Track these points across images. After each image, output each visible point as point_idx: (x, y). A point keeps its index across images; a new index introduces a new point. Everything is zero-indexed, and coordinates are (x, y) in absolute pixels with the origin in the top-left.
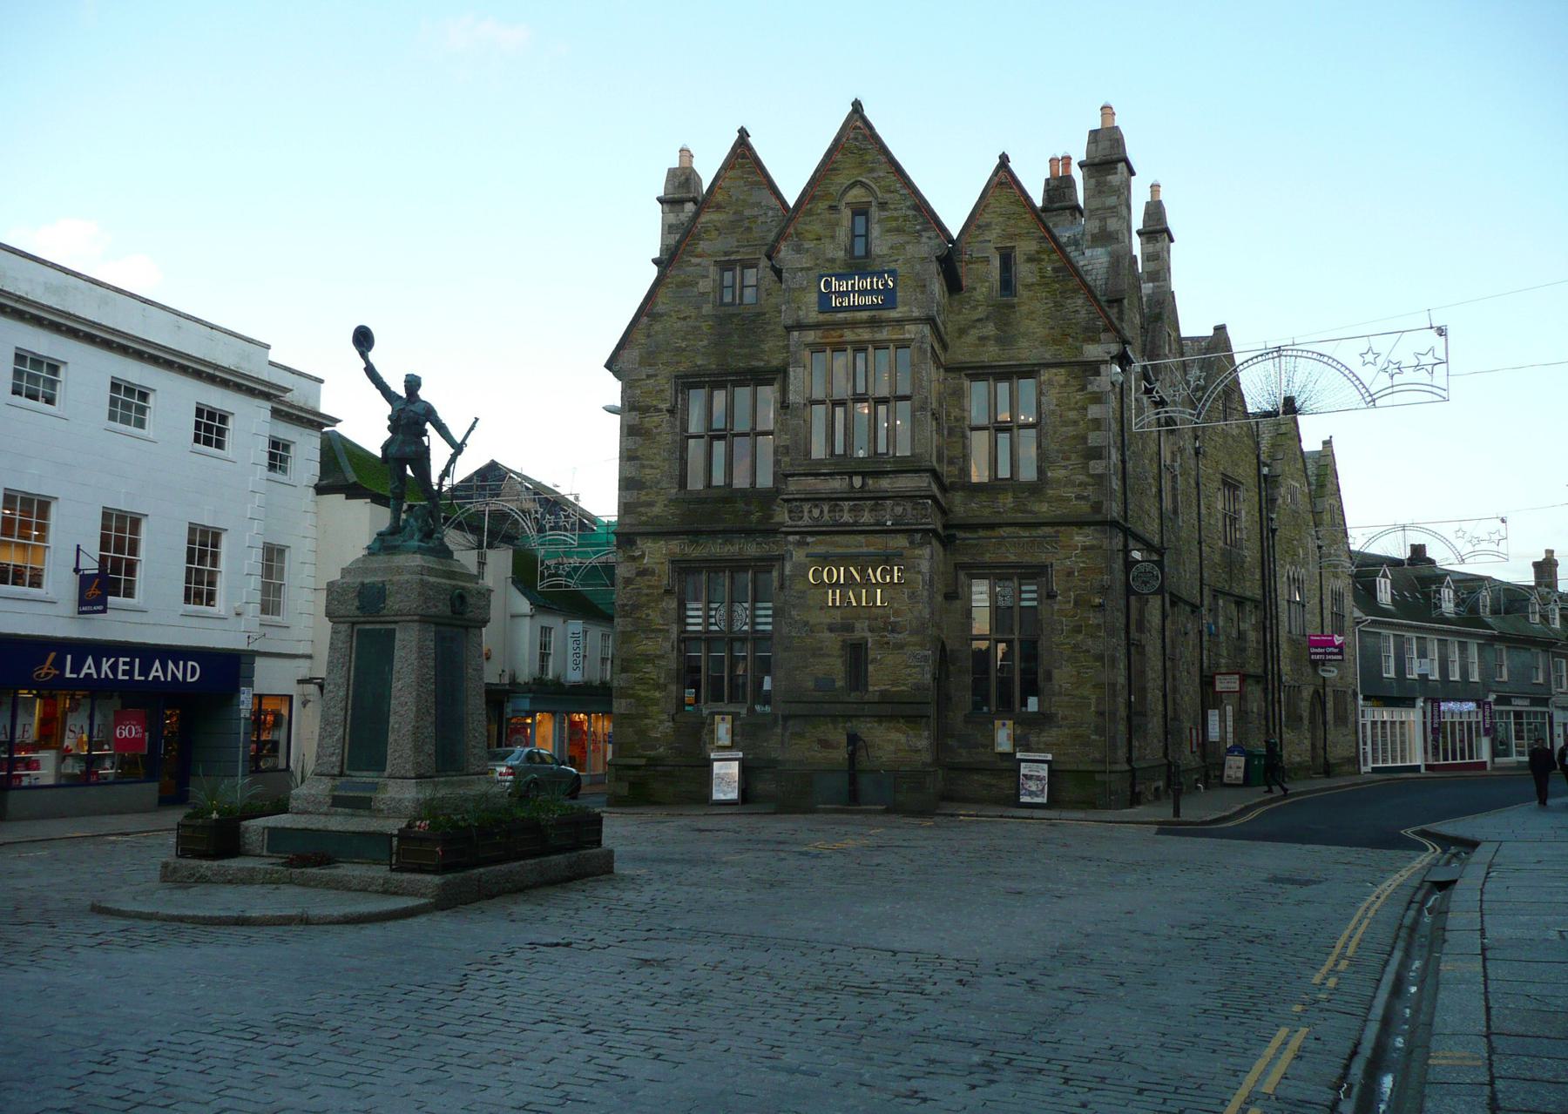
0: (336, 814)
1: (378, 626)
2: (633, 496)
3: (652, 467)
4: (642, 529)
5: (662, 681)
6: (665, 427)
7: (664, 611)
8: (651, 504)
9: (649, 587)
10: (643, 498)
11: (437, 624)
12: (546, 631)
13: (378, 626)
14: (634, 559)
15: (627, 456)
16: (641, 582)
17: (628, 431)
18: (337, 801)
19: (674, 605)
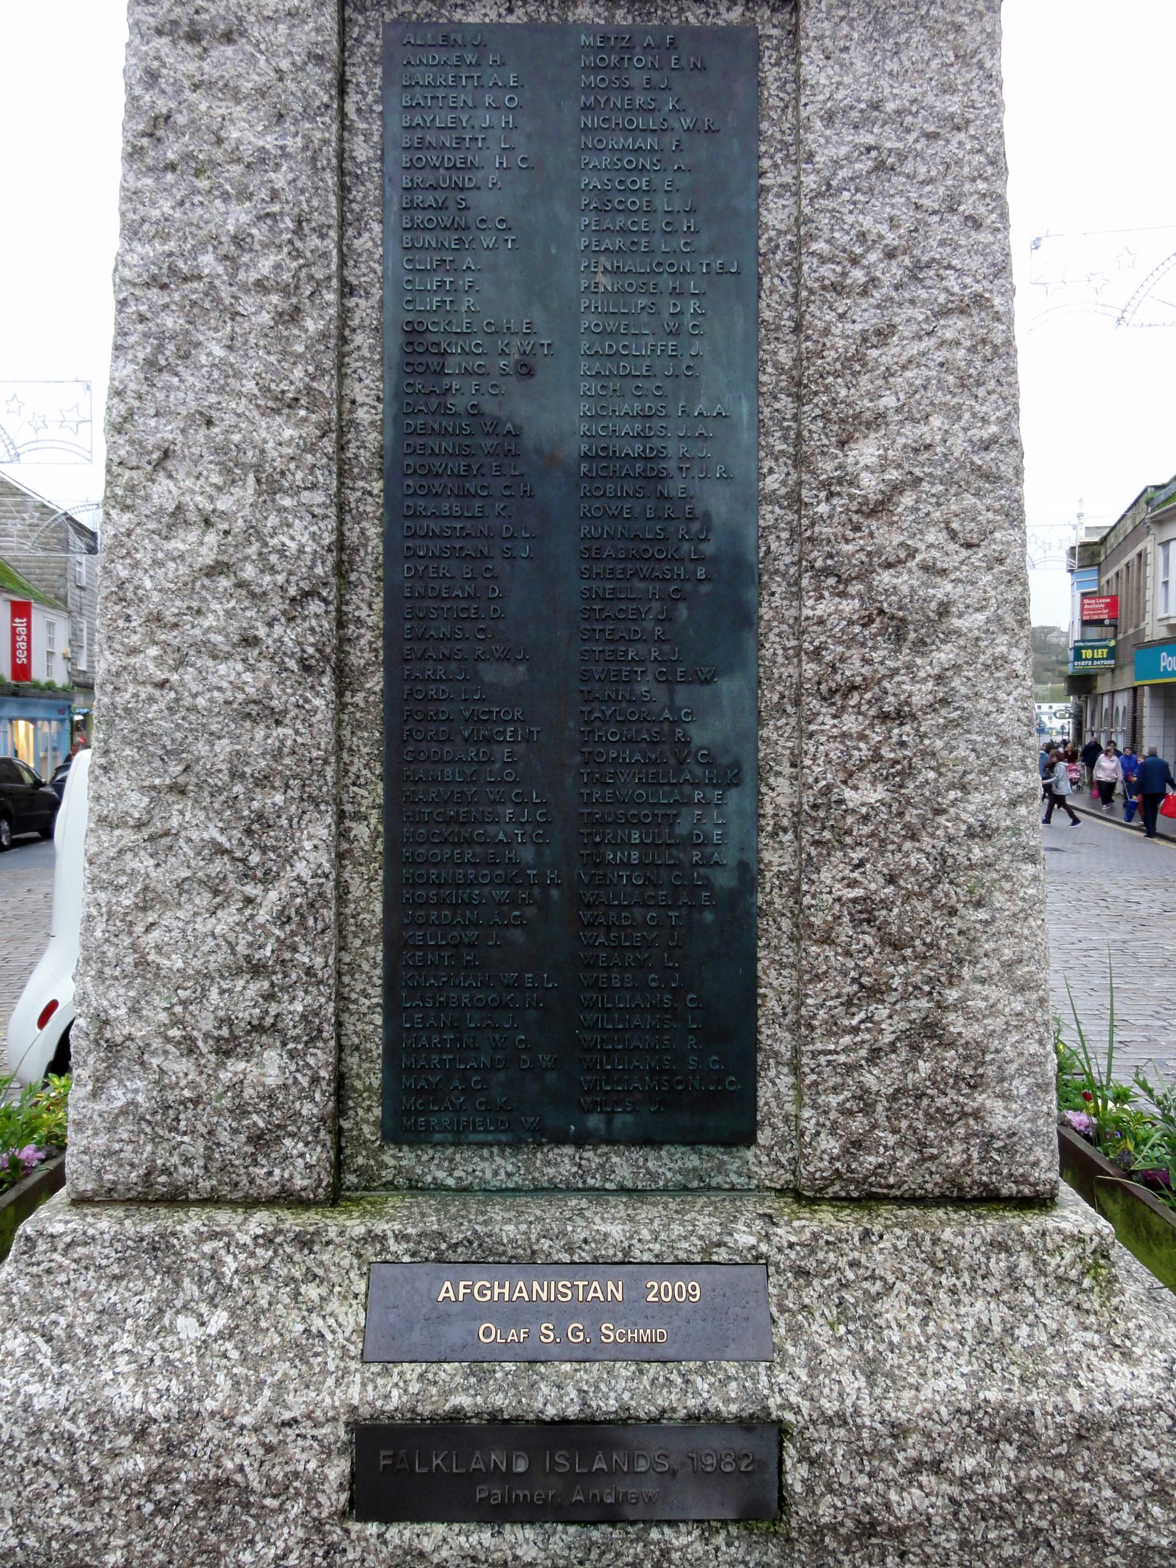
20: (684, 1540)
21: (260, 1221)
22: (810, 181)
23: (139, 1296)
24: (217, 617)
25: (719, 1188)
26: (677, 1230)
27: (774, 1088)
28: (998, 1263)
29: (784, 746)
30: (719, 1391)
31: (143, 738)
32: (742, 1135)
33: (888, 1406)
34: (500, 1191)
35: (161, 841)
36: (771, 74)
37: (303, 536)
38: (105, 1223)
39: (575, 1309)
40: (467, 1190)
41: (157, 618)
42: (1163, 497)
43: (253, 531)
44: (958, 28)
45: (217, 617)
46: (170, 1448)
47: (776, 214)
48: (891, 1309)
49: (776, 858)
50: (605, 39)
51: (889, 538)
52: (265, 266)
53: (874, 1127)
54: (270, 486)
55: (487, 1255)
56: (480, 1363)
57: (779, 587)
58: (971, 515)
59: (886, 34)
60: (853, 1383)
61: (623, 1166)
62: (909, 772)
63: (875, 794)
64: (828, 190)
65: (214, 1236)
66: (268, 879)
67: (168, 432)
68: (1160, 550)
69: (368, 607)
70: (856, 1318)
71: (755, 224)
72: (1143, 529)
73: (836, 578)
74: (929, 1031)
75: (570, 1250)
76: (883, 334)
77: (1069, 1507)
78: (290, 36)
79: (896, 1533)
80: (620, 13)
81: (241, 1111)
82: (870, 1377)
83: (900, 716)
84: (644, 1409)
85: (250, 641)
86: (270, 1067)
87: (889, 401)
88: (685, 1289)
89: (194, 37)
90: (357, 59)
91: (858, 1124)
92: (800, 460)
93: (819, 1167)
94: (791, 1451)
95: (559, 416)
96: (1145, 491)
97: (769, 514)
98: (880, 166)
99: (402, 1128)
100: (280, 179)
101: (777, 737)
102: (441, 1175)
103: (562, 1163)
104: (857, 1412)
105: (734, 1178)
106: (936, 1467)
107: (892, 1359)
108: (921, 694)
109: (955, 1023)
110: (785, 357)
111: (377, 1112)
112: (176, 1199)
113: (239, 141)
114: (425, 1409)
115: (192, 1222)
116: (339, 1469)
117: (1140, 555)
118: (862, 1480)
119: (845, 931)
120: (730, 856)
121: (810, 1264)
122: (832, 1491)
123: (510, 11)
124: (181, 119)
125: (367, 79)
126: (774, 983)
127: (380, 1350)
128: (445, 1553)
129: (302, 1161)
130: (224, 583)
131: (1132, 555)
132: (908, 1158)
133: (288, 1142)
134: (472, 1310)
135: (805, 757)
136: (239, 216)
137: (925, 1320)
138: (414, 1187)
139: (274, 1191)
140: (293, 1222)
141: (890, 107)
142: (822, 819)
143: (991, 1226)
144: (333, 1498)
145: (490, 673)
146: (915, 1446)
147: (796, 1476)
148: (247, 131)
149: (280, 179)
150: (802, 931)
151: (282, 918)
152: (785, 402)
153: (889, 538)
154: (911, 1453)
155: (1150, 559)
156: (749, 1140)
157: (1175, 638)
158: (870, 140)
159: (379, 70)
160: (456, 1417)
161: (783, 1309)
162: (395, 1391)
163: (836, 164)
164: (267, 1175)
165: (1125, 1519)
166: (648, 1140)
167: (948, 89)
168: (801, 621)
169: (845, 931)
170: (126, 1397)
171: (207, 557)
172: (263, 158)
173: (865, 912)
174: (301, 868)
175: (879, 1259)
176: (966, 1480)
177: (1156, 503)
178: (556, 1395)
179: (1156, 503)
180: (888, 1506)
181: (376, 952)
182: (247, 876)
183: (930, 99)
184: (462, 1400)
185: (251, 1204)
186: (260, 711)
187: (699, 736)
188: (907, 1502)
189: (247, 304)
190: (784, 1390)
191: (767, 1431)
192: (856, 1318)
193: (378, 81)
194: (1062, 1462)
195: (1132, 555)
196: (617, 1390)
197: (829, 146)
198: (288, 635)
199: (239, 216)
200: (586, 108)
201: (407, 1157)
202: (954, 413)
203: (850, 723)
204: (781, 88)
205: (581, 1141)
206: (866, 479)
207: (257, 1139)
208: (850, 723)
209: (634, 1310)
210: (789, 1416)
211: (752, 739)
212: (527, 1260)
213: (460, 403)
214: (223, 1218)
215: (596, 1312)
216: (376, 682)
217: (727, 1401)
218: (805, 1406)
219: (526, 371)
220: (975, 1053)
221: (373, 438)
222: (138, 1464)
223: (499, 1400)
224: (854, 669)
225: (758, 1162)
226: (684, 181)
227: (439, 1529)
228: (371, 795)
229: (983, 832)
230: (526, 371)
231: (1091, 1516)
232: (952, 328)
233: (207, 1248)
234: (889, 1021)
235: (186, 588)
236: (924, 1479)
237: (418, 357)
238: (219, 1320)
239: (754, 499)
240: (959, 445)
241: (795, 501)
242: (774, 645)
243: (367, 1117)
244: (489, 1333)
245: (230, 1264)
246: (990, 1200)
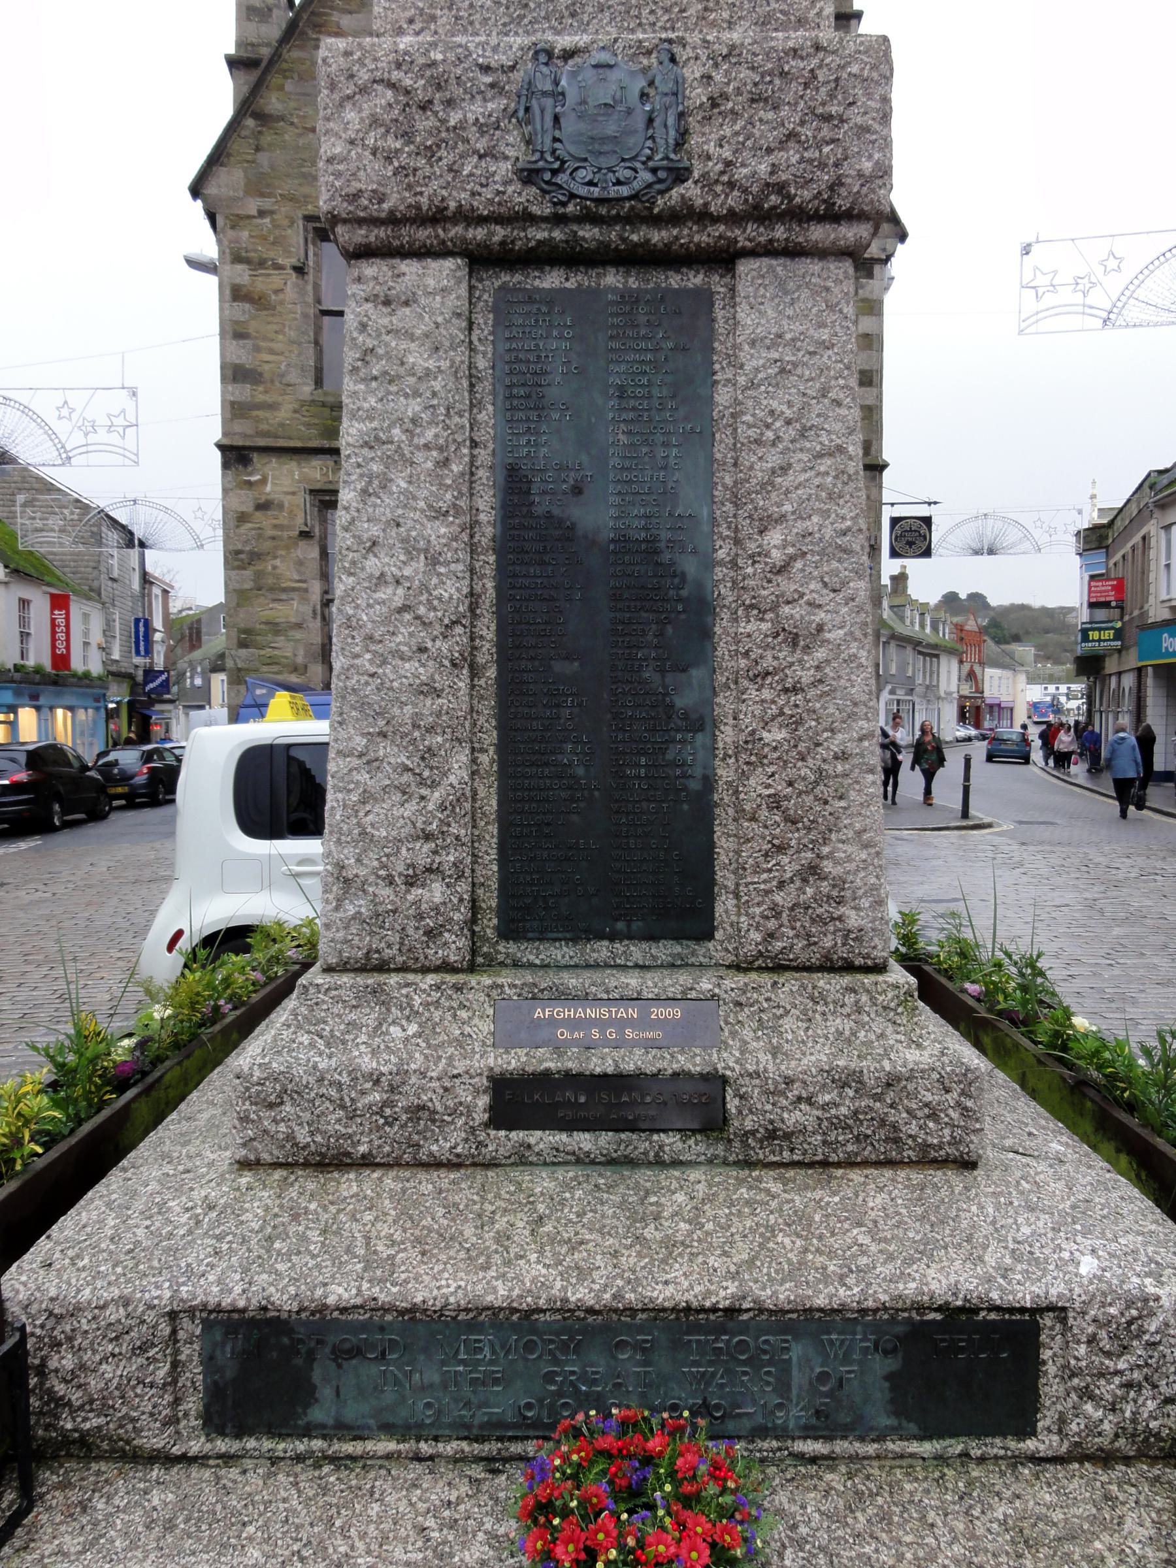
0: (522, 1159)
2: (244, 392)
3: (272, 352)
4: (262, 442)
5: (300, 660)
6: (290, 293)
7: (300, 563)
8: (273, 407)
9: (275, 526)
10: (261, 398)
12: (24, 603)
14: (250, 484)
15: (233, 332)
16: (264, 520)
17: (235, 294)
19: (315, 553)
20: (672, 1140)
21: (431, 979)
22: (742, 380)
23: (369, 1016)
24: (404, 635)
25: (693, 965)
26: (668, 982)
27: (724, 906)
28: (850, 999)
29: (730, 708)
30: (692, 1061)
31: (363, 705)
32: (706, 933)
33: (783, 1067)
34: (566, 967)
35: (373, 764)
36: (719, 314)
37: (451, 590)
38: (346, 979)
39: (611, 1022)
40: (548, 966)
41: (371, 638)
42: (1165, 482)
43: (424, 588)
44: (828, 289)
45: (404, 635)
46: (392, 1089)
47: (723, 396)
48: (787, 1023)
49: (725, 773)
50: (622, 297)
51: (788, 586)
52: (430, 434)
53: (781, 926)
54: (433, 561)
55: (562, 996)
56: (558, 1049)
57: (725, 615)
58: (836, 573)
59: (786, 293)
60: (765, 1058)
61: (637, 951)
62: (800, 722)
64: (752, 385)
65: (407, 985)
66: (434, 785)
67: (375, 531)
68: (1162, 533)
69: (487, 629)
70: (768, 1027)
71: (710, 401)
72: (1146, 513)
73: (757, 609)
74: (812, 871)
75: (608, 992)
76: (785, 469)
77: (883, 1122)
78: (443, 303)
79: (788, 1136)
80: (631, 280)
81: (420, 917)
82: (774, 1056)
83: (795, 690)
84: (650, 1069)
85: (422, 650)
86: (436, 892)
87: (788, 508)
88: (674, 1012)
89: (387, 302)
90: (478, 309)
91: (772, 924)
92: (737, 542)
93: (750, 949)
94: (729, 1092)
95: (598, 517)
96: (1149, 475)
97: (719, 572)
98: (783, 371)
99: (510, 930)
100: (437, 385)
101: (725, 703)
102: (532, 957)
103: (601, 950)
104: (766, 1070)
105: (702, 959)
106: (809, 1101)
107: (787, 1047)
108: (807, 676)
109: (828, 866)
110: (728, 480)
111: (495, 921)
112: (382, 967)
113: (414, 364)
114: (530, 1069)
115: (394, 979)
116: (484, 1101)
117: (1144, 538)
118: (769, 1107)
119: (764, 813)
120: (698, 772)
121: (743, 999)
122: (751, 1112)
123: (567, 279)
124: (381, 351)
125: (485, 322)
126: (724, 845)
127: (503, 1040)
128: (541, 1146)
129: (454, 947)
130: (407, 616)
131: (1137, 538)
132: (801, 943)
133: (446, 935)
134: (552, 1022)
135: (741, 713)
136: (414, 407)
137: (807, 1029)
138: (516, 964)
139: (439, 962)
140: (451, 979)
141: (788, 336)
142: (752, 751)
143: (846, 980)
144: (480, 1116)
145: (558, 667)
146: (797, 1090)
147: (732, 1104)
148: (419, 358)
149: (437, 385)
150: (740, 811)
151: (442, 807)
152: (729, 506)
153: (788, 586)
154: (796, 1093)
155: (1153, 542)
156: (710, 937)
157: (1175, 620)
158: (776, 356)
159: (491, 316)
160: (547, 1074)
161: (727, 1023)
162: (514, 1061)
163: (757, 370)
164: (435, 954)
165: (913, 1129)
166: (652, 937)
167: (822, 325)
168: (737, 634)
169: (764, 813)
170: (367, 1063)
171: (398, 602)
172: (428, 373)
173: (775, 803)
174: (452, 779)
175: (782, 996)
176: (825, 1107)
177: (1158, 487)
178: (601, 1063)
179: (1158, 487)
180: (783, 1121)
181: (494, 829)
182: (422, 783)
183: (811, 331)
184: (551, 1065)
185: (425, 970)
186: (429, 690)
187: (680, 702)
188: (792, 1119)
189: (419, 457)
190: (726, 1061)
191: (717, 1081)
192: (768, 1027)
193: (490, 322)
194: (878, 1098)
195: (1137, 538)
196: (633, 1061)
197: (753, 360)
198: (444, 646)
199: (414, 407)
200: (611, 337)
201: (512, 947)
202: (825, 514)
203: (767, 694)
204: (726, 322)
205: (612, 938)
206: (775, 553)
207: (429, 933)
208: (767, 694)
209: (644, 1022)
210: (728, 1073)
211: (711, 704)
212: (584, 998)
213: (539, 510)
214: (411, 977)
215: (622, 1024)
216: (492, 672)
217: (695, 1065)
218: (737, 1068)
219: (577, 490)
220: (839, 883)
221: (489, 531)
222: (377, 1097)
223: (570, 1065)
224: (768, 663)
225: (715, 949)
226: (669, 379)
227: (539, 1133)
228: (490, 738)
229: (843, 756)
230: (577, 490)
231: (895, 1128)
232: (825, 464)
233: (404, 991)
234: (789, 865)
235: (386, 621)
236: (802, 1107)
237: (515, 485)
238: (413, 1028)
239: (710, 563)
240: (828, 533)
241: (734, 564)
242: (722, 650)
243: (489, 924)
244: (563, 1034)
245: (417, 1001)
246: (849, 967)
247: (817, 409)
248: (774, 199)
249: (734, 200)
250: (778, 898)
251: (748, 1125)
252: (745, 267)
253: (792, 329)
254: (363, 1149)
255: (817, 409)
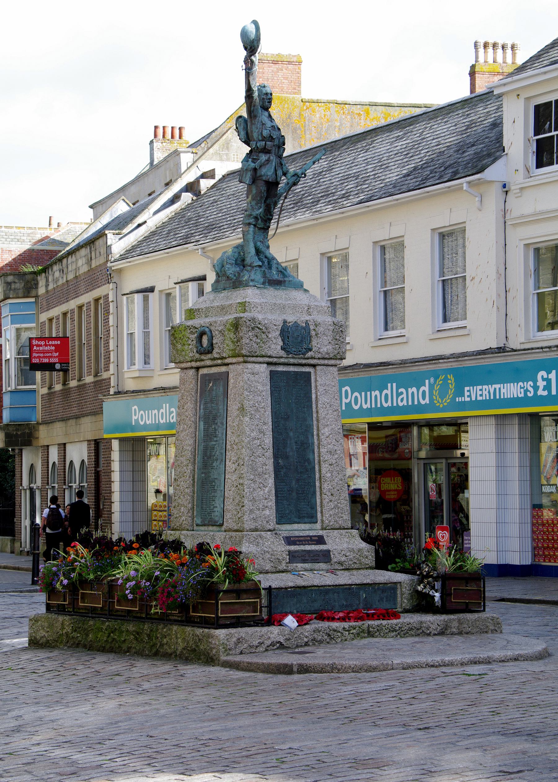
1: (292, 369)
11: (269, 364)
13: (292, 369)
18: (293, 557)
28: (347, 535)
63: (330, 475)
67: (253, 427)
94: (331, 553)
100: (264, 393)
130: (260, 447)
136: (260, 398)
146: (343, 553)
147: (332, 556)
148: (260, 387)
151: (268, 492)
167: (333, 382)
203: (327, 466)
206: (327, 433)
224: (326, 458)
247: (333, 401)
248: (327, 356)
249: (320, 356)
250: (331, 512)
251: (335, 560)
252: (318, 368)
253: (328, 382)
254: (267, 568)
255: (333, 401)
